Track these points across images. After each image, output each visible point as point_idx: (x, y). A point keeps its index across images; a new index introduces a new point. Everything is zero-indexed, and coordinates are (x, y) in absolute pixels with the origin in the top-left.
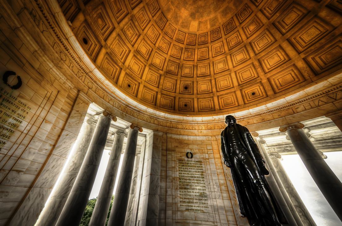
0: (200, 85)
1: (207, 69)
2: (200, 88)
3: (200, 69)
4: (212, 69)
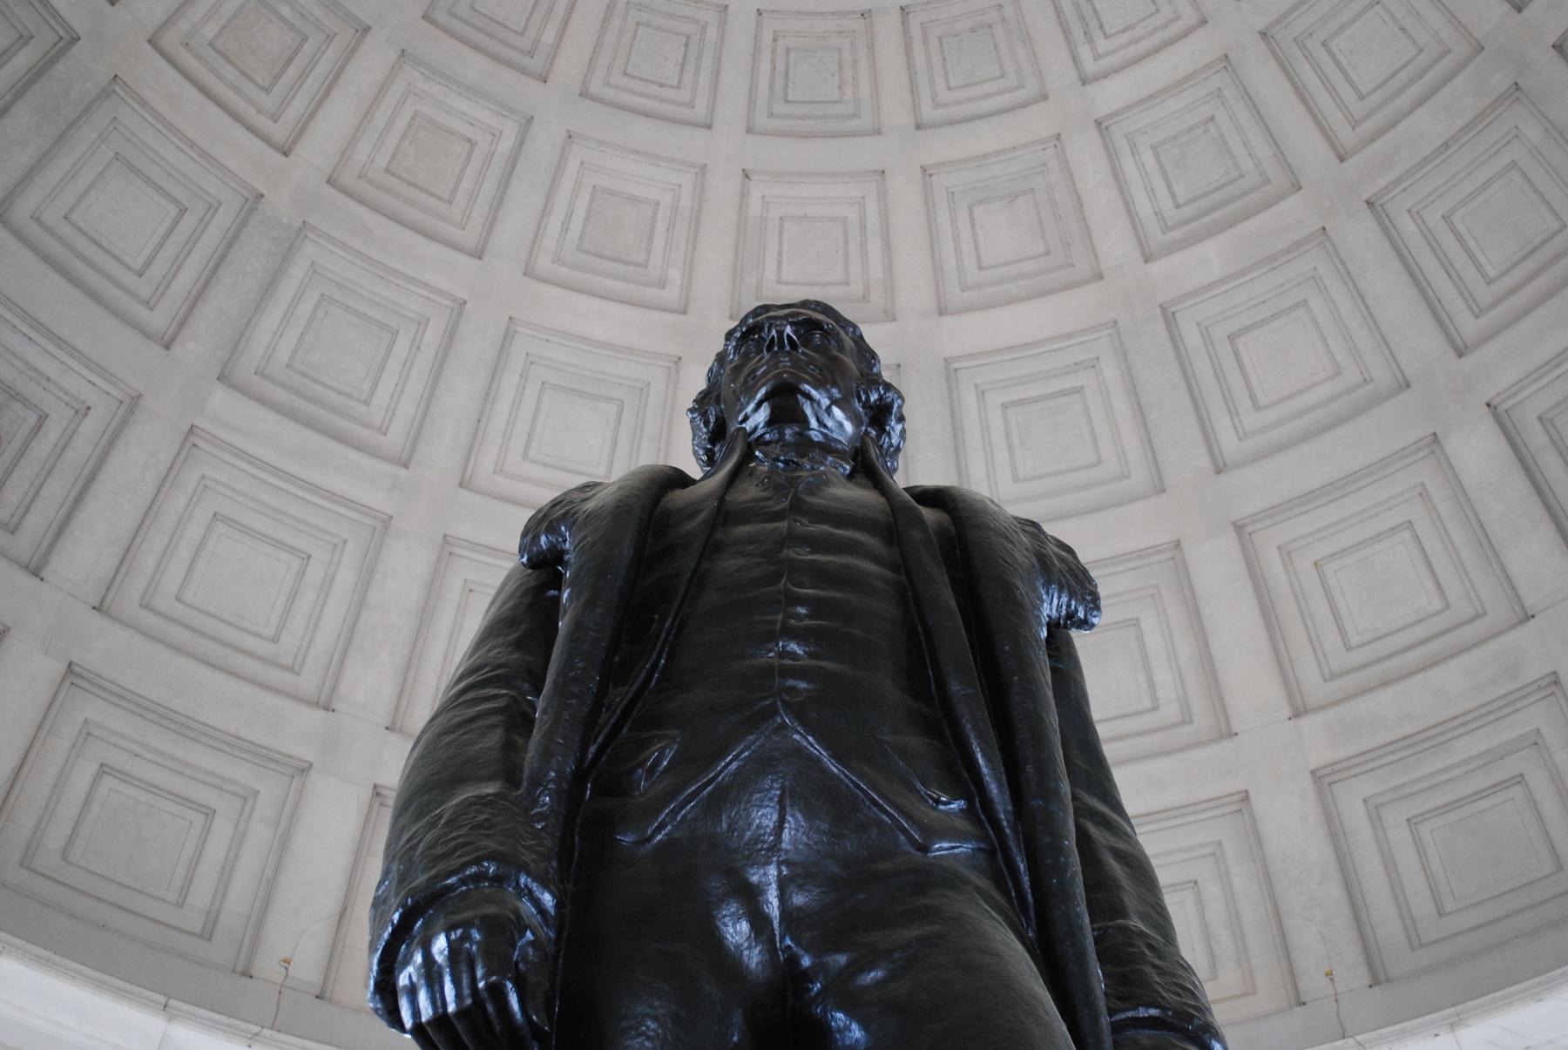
0: (202, 517)
1: (394, 364)
2: (184, 552)
3: (304, 310)
4: (459, 396)
